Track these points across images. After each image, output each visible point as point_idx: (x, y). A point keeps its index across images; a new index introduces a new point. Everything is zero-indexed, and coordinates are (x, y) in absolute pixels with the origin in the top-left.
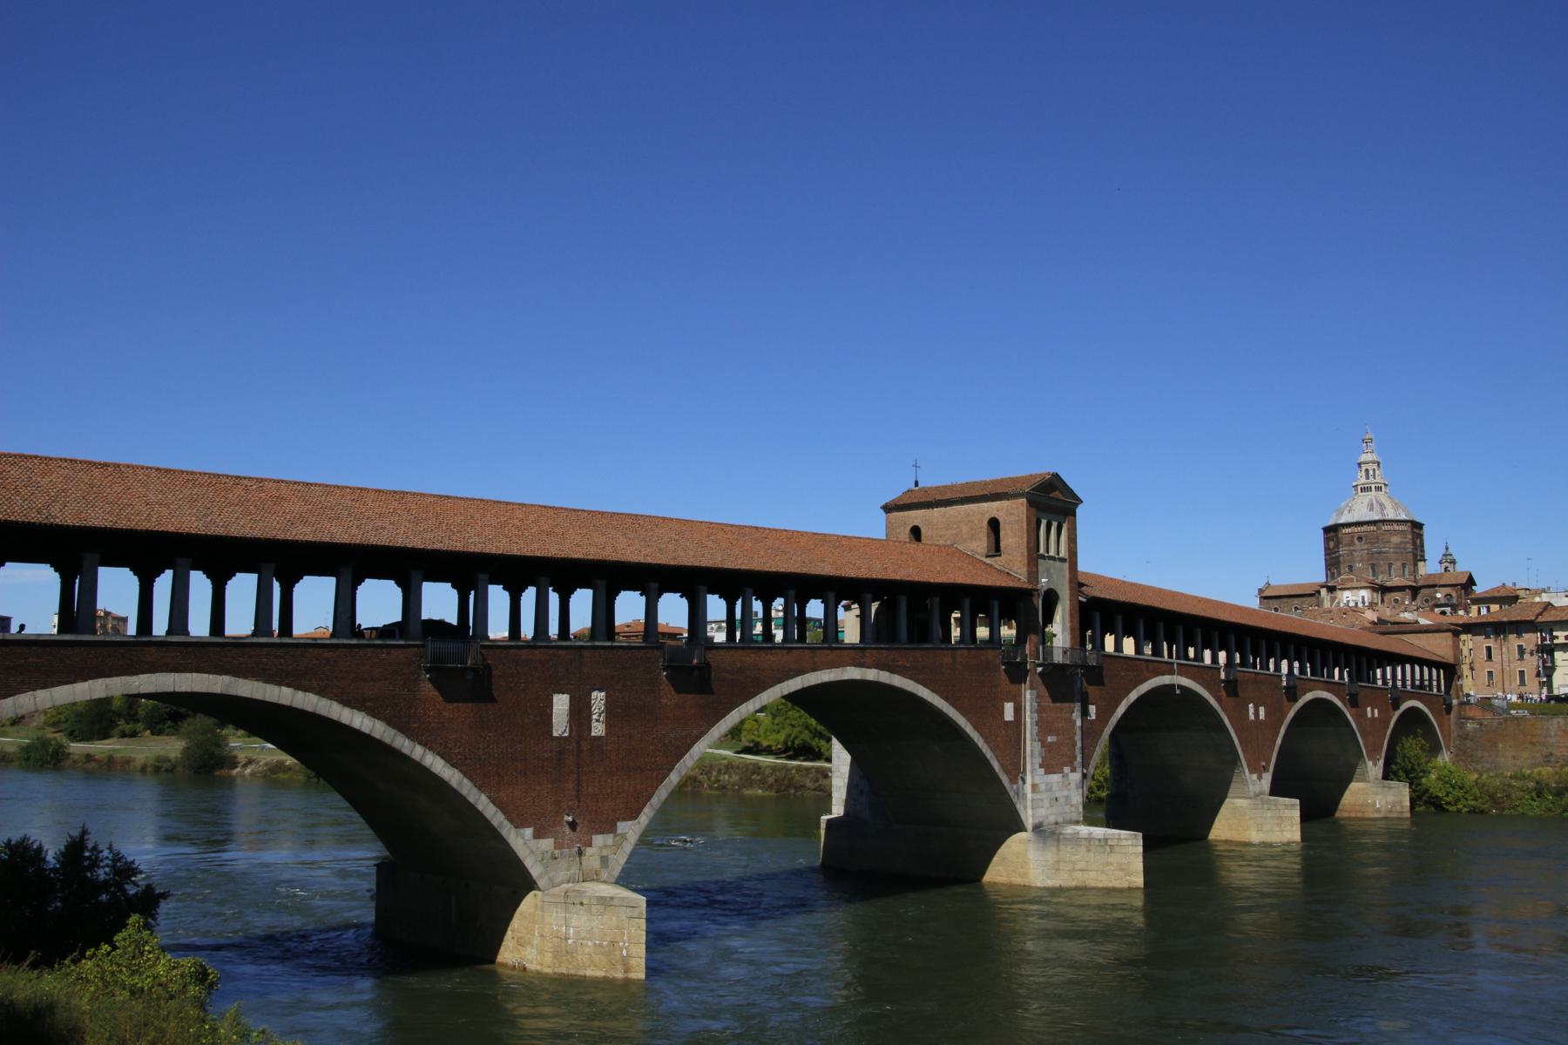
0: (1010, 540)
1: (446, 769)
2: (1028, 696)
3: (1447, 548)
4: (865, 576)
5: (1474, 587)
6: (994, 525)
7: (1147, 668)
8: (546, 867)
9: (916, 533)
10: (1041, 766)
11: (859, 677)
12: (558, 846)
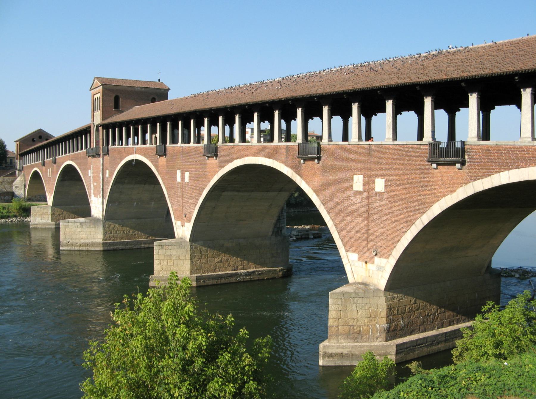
7: (125, 151)
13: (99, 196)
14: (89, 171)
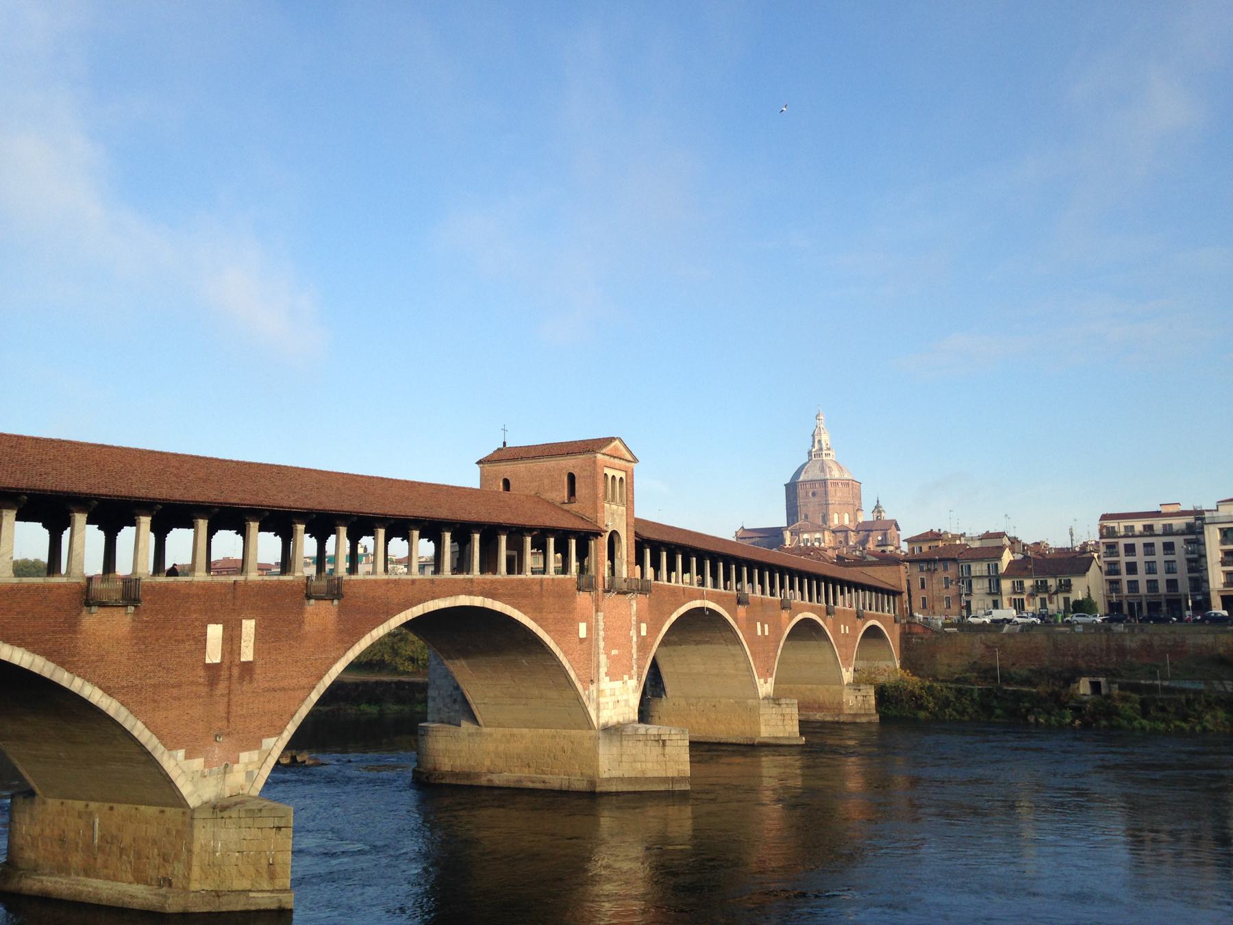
0: (583, 491)
1: (104, 699)
3: (878, 502)
4: (476, 520)
5: (898, 532)
6: (572, 478)
7: (684, 593)
8: (195, 784)
9: (507, 483)
10: (607, 674)
11: (468, 604)
12: (207, 764)
13: (626, 677)
14: (583, 627)
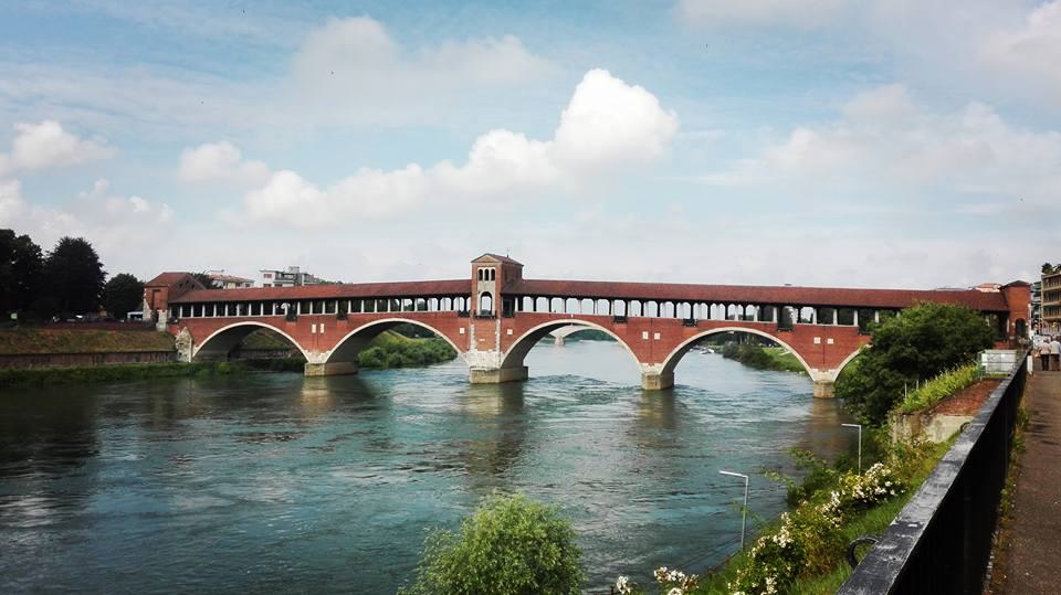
2: (472, 327)
